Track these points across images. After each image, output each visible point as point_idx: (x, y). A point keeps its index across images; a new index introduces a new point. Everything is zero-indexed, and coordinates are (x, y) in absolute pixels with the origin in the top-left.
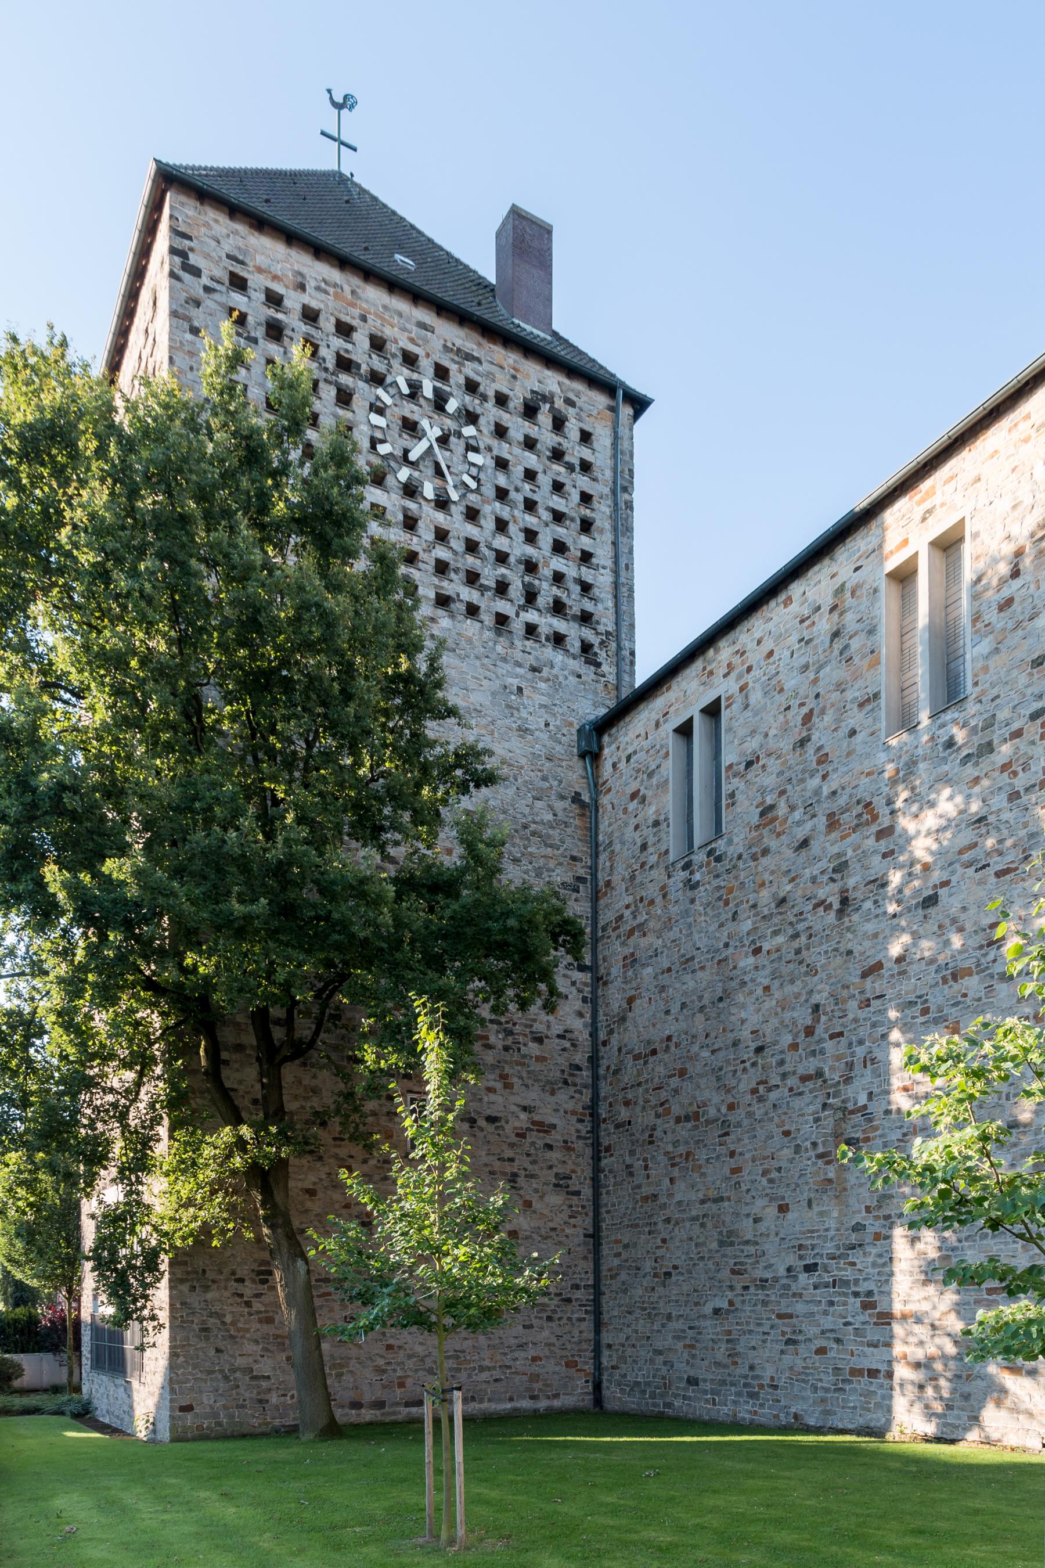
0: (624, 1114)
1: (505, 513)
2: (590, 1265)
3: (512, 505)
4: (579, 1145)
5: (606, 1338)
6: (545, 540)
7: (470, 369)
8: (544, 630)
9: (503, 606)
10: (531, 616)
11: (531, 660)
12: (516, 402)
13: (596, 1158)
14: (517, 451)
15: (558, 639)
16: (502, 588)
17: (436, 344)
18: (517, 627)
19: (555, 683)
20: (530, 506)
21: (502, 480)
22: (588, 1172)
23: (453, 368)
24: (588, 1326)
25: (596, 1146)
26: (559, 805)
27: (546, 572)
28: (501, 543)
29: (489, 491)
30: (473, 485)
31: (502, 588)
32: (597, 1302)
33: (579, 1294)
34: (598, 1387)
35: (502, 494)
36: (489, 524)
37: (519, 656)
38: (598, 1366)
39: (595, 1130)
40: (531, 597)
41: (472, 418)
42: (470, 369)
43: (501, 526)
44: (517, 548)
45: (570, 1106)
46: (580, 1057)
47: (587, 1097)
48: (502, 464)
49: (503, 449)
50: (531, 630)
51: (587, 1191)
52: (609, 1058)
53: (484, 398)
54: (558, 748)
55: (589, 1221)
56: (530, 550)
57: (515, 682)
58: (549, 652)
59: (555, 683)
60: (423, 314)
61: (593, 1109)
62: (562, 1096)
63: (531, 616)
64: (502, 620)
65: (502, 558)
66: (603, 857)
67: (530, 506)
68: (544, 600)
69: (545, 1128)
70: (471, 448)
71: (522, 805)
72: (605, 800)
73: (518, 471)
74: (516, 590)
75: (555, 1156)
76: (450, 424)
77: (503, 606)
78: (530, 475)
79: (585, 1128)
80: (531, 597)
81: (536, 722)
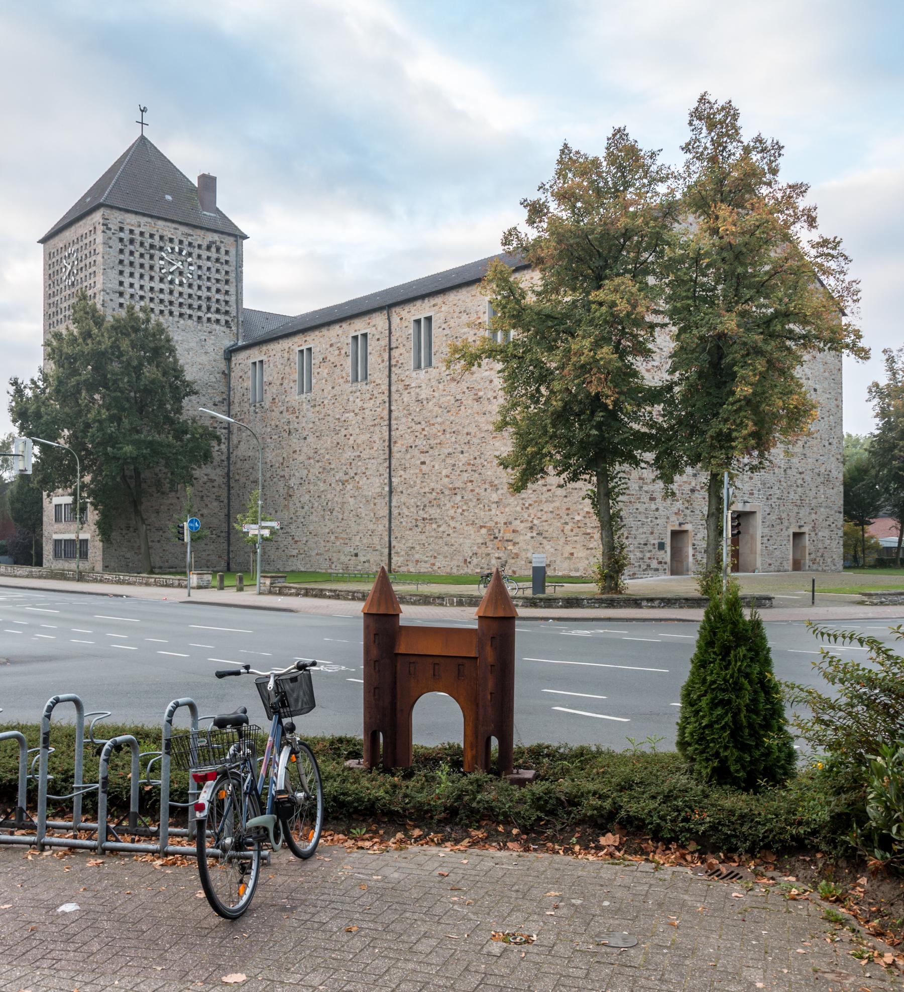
0: (237, 477)
1: (200, 283)
2: (226, 525)
3: (203, 280)
4: (223, 486)
5: (231, 549)
6: (214, 290)
7: (190, 239)
8: (213, 319)
9: (200, 314)
10: (209, 315)
11: (209, 330)
12: (204, 246)
13: (229, 490)
14: (205, 262)
15: (218, 321)
16: (200, 308)
17: (179, 232)
18: (205, 320)
19: (217, 336)
20: (209, 279)
21: (200, 273)
22: (226, 495)
23: (184, 240)
24: (225, 545)
25: (229, 486)
26: (218, 375)
27: (214, 300)
28: (199, 293)
29: (196, 277)
30: (190, 276)
31: (200, 308)
32: (228, 537)
33: (223, 534)
34: (228, 564)
35: (199, 277)
36: (195, 288)
37: (205, 329)
38: (229, 558)
39: (228, 481)
40: (209, 308)
41: (190, 254)
42: (190, 239)
43: (199, 287)
44: (204, 293)
45: (221, 473)
46: (224, 457)
47: (226, 471)
48: (200, 267)
49: (200, 263)
50: (209, 320)
51: (226, 501)
52: (233, 459)
53: (194, 247)
54: (218, 357)
55: (226, 511)
56: (209, 294)
57: (203, 338)
58: (215, 326)
59: (217, 336)
60: (174, 225)
61: (228, 474)
62: (218, 470)
63: (209, 315)
64: (199, 318)
65: (199, 298)
66: (232, 393)
67: (209, 279)
68: (213, 309)
69: (212, 481)
70: (190, 264)
71: (206, 377)
72: (232, 374)
73: (205, 268)
74: (204, 308)
75: (215, 490)
76: (183, 258)
77: (200, 314)
78: (209, 269)
79: (225, 480)
80: (209, 308)
81: (210, 350)
